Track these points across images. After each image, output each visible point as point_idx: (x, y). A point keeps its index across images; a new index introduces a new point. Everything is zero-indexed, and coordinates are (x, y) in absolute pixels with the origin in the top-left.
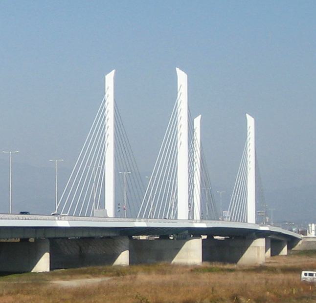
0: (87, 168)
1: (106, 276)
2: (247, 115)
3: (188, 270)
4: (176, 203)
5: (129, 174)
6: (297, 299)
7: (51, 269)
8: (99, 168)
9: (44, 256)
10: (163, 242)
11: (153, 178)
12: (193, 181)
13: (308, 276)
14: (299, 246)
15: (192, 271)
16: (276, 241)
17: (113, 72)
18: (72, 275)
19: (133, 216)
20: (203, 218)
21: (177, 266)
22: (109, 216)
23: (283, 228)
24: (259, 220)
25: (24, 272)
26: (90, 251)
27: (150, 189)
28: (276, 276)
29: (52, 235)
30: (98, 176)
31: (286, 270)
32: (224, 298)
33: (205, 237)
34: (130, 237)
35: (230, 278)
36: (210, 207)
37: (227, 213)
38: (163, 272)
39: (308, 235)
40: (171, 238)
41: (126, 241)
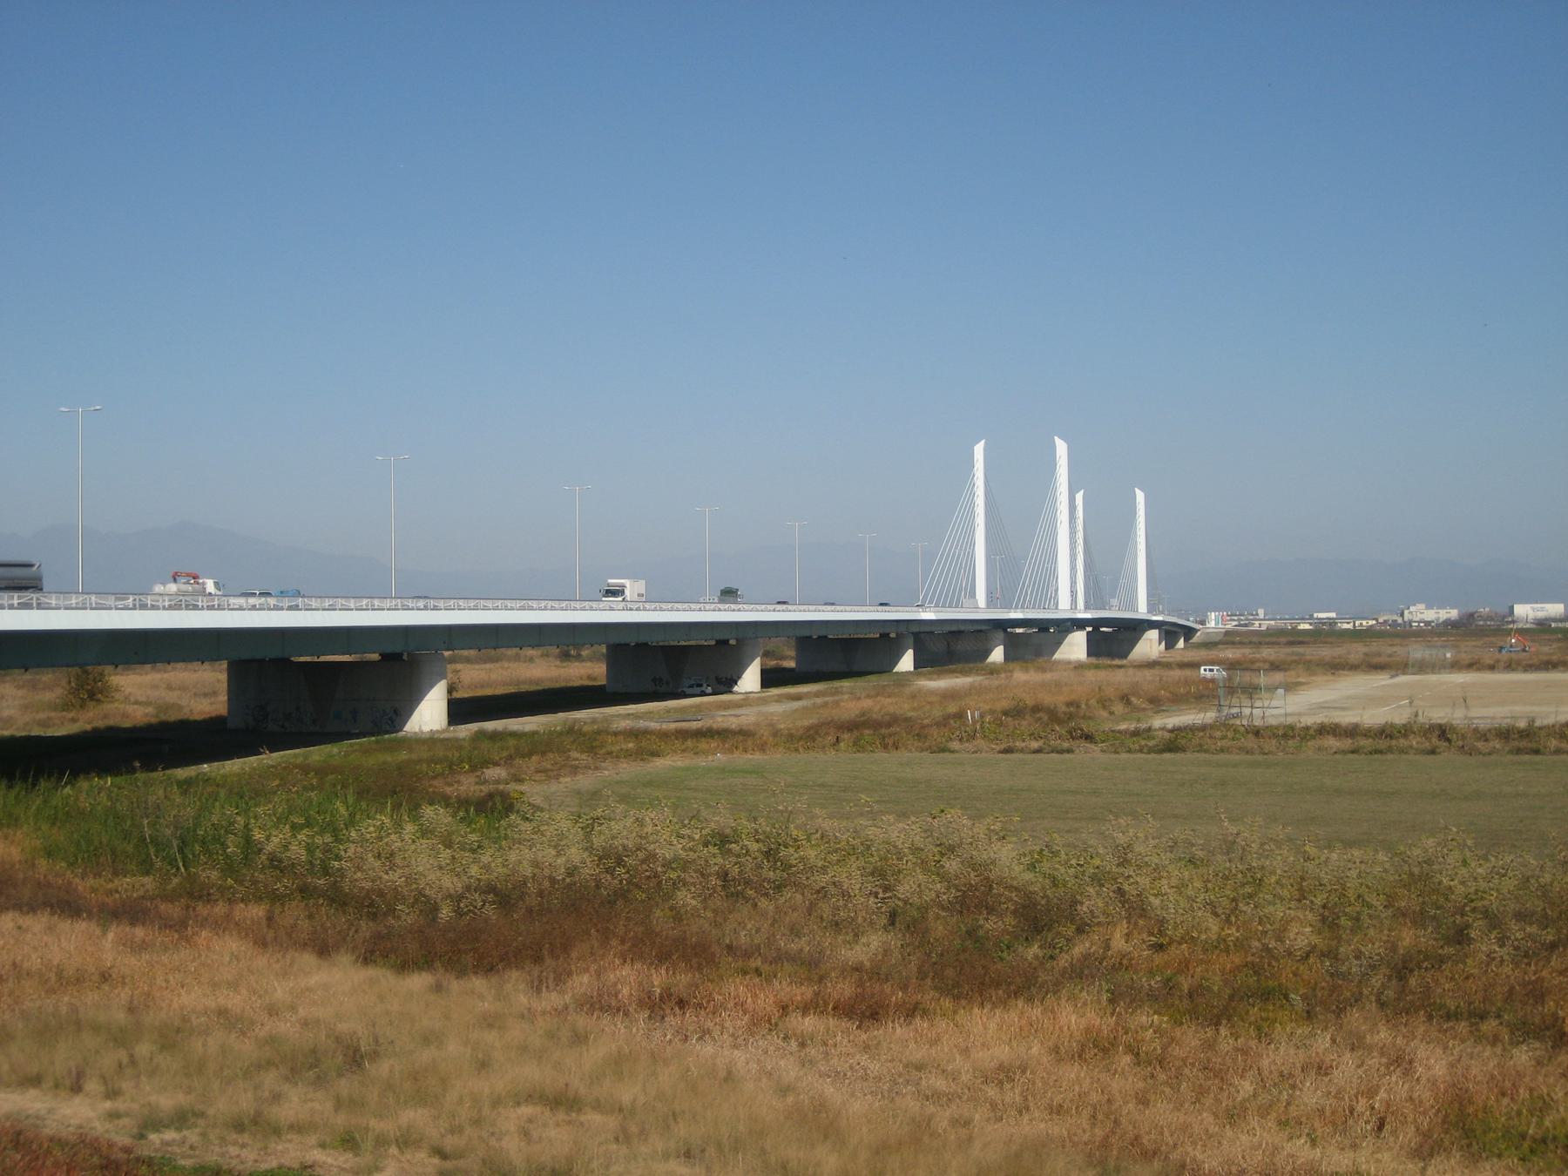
0: (955, 552)
1: (978, 675)
2: (1137, 490)
3: (1072, 666)
4: (1057, 591)
5: (1002, 558)
6: (1196, 698)
7: (915, 668)
8: (969, 553)
9: (906, 654)
10: (1042, 635)
11: (1030, 563)
12: (1076, 565)
13: (1208, 672)
14: (1197, 638)
15: (1075, 667)
16: (1171, 633)
17: (983, 442)
18: (940, 675)
19: (1008, 606)
20: (1087, 608)
21: (1059, 662)
22: (980, 606)
23: (1178, 618)
24: (1152, 608)
25: (885, 672)
26: (959, 647)
27: (1026, 575)
28: (1172, 673)
29: (915, 629)
30: (967, 561)
31: (1183, 665)
32: (1112, 698)
33: (1090, 629)
34: (1005, 631)
35: (1119, 677)
36: (1095, 595)
37: (1114, 602)
38: (1044, 670)
39: (1208, 625)
40: (1052, 631)
41: (1000, 635)
